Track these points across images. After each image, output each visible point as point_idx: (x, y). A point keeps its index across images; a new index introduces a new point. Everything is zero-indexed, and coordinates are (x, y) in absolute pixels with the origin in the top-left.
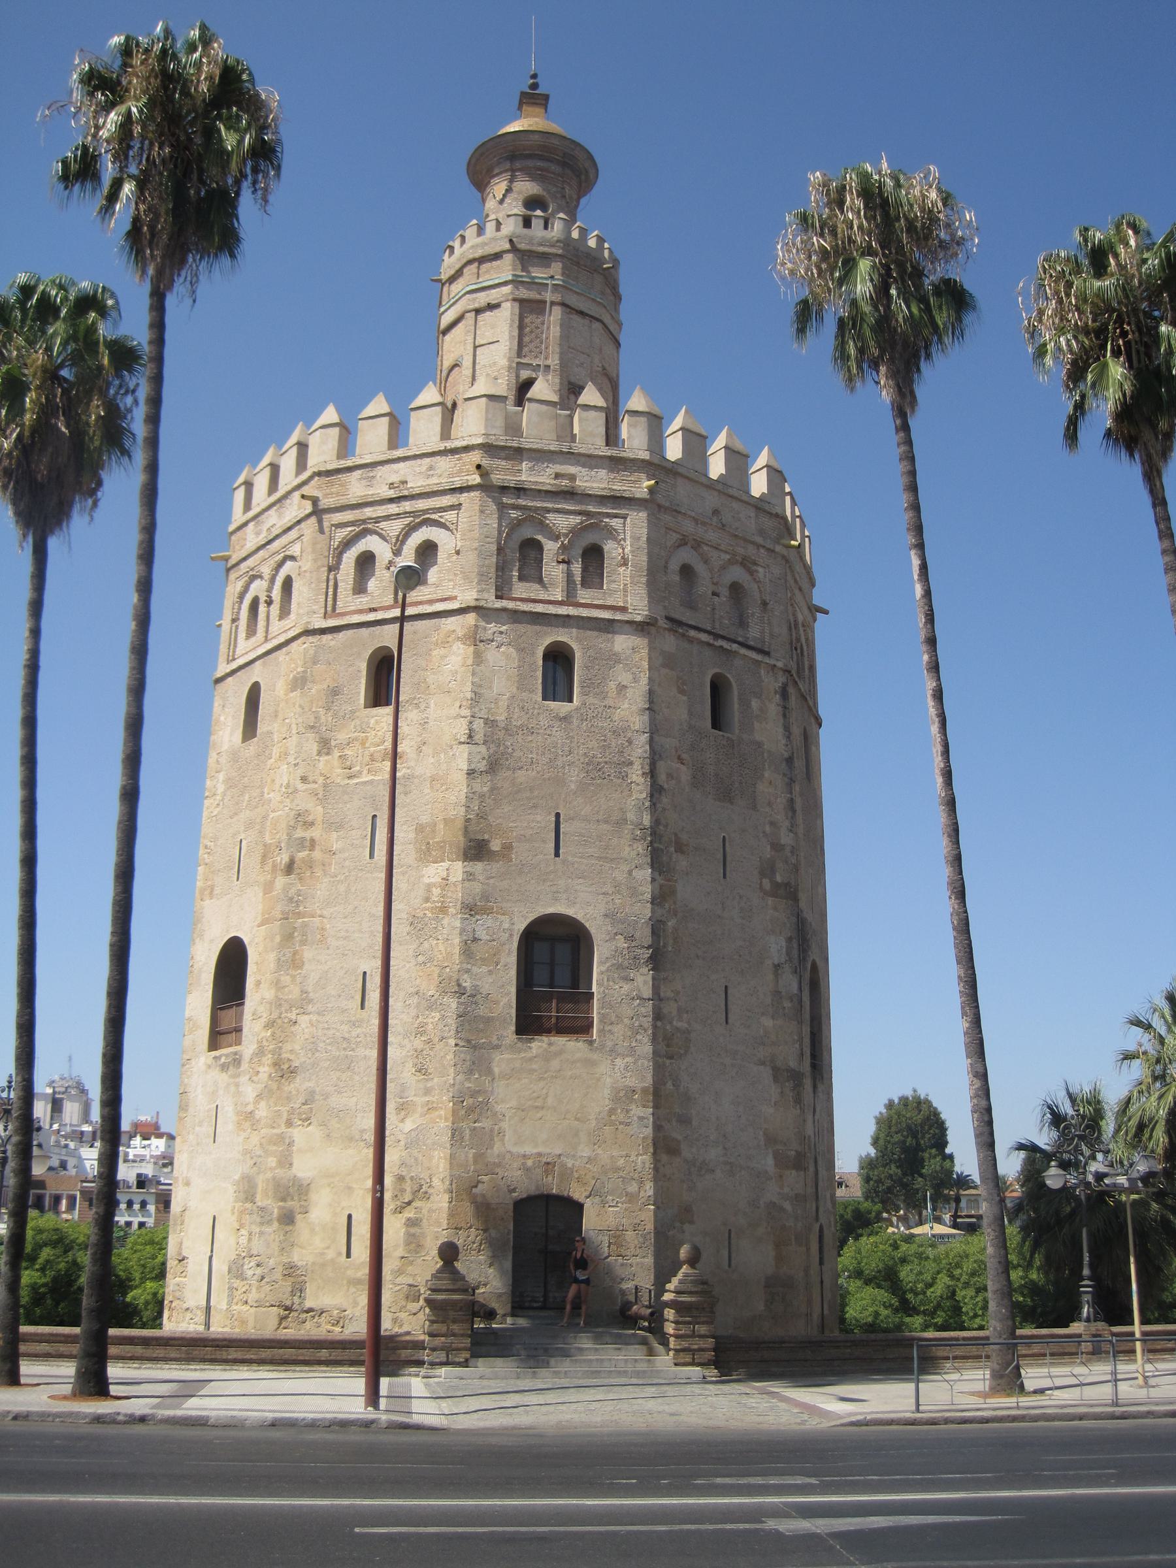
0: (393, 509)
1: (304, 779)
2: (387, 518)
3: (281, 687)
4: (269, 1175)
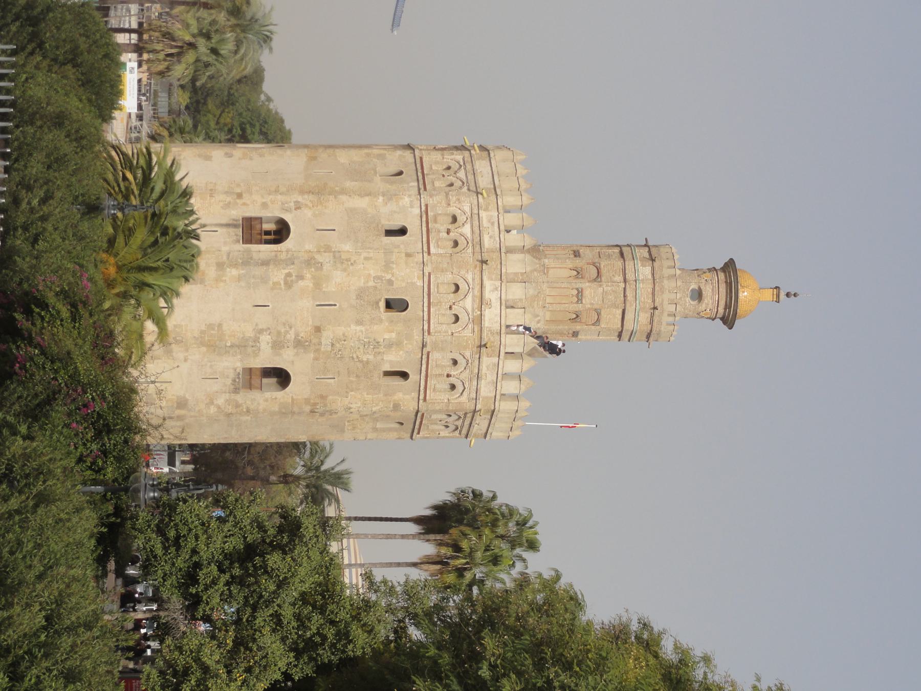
2: (463, 422)
3: (399, 396)
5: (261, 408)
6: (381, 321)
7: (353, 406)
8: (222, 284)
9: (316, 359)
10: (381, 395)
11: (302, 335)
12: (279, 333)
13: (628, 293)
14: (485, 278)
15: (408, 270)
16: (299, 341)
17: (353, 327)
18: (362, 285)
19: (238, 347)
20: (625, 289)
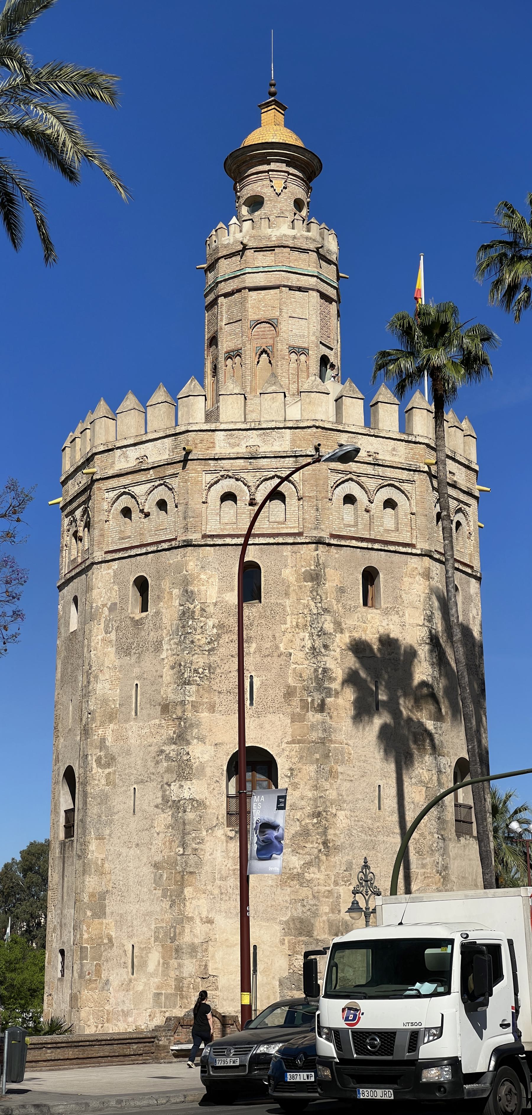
0: (370, 470)
1: (326, 647)
2: (367, 475)
3: (288, 574)
4: (325, 918)
5: (310, 795)
6: (158, 613)
7: (309, 644)
8: (106, 865)
9: (212, 708)
10: (288, 602)
11: (171, 733)
12: (168, 770)
13: (228, 289)
14: (110, 473)
15: (100, 585)
16: (179, 736)
17: (164, 655)
18: (114, 649)
19: (184, 834)
20: (226, 295)
